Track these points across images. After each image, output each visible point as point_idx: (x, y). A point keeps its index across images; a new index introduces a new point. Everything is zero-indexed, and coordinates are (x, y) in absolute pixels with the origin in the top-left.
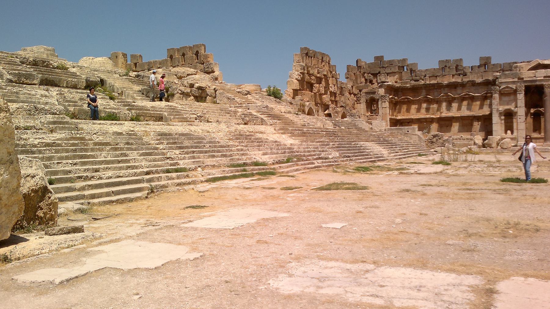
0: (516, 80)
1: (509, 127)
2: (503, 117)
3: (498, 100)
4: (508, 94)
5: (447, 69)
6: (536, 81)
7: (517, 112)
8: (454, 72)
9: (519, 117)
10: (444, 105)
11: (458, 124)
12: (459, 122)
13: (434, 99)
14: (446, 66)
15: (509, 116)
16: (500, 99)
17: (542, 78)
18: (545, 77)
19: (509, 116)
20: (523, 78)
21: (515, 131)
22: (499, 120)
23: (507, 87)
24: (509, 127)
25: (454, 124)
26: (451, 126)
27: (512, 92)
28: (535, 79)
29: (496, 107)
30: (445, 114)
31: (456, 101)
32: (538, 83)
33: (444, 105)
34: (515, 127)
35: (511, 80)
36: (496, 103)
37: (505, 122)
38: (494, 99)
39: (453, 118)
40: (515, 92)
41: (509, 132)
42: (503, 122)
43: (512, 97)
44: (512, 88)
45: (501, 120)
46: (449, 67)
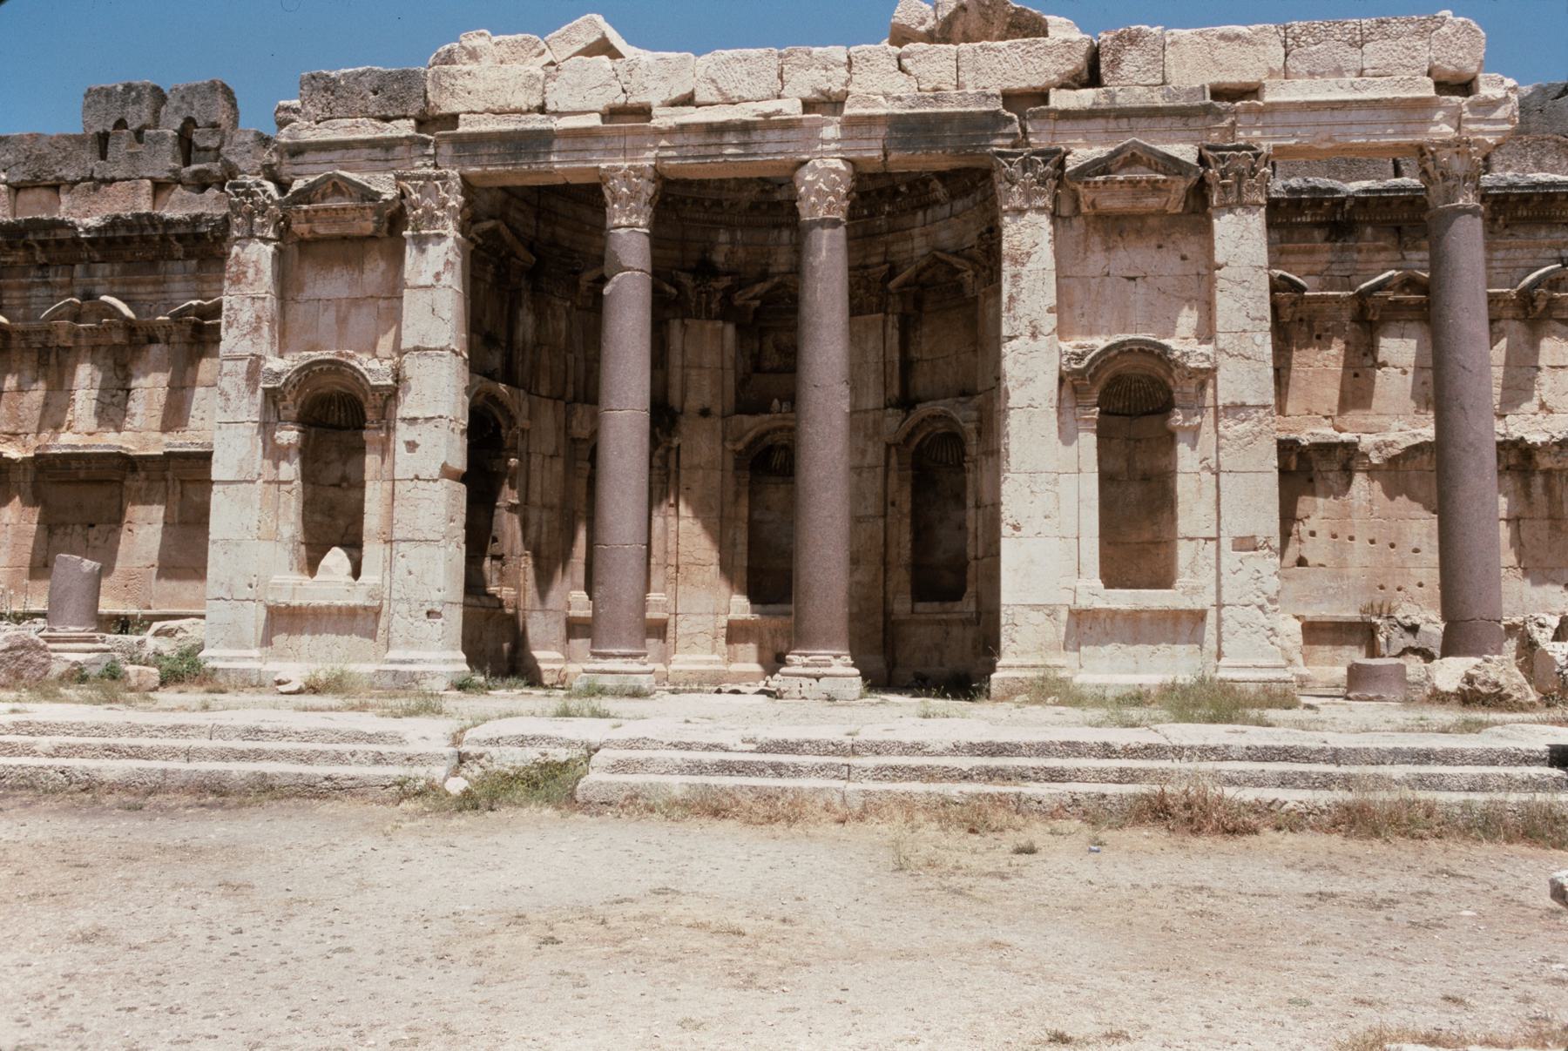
0: (405, 128)
1: (332, 523)
2: (289, 435)
3: (264, 283)
4: (346, 249)
5: (121, 147)
6: (541, 141)
7: (391, 395)
8: (165, 162)
9: (403, 433)
10: (86, 379)
11: (158, 512)
12: (165, 500)
13: (25, 335)
14: (121, 124)
15: (333, 424)
16: (286, 284)
17: (594, 121)
18: (612, 114)
19: (333, 424)
20: (453, 119)
21: (372, 551)
22: (260, 464)
23: (337, 186)
24: (332, 523)
25: (136, 512)
26: (117, 520)
27: (368, 227)
28: (536, 122)
29: (245, 347)
30: (81, 431)
31: (155, 351)
32: (560, 165)
33: (86, 379)
34: (372, 520)
35: (368, 130)
36: (246, 315)
37: (308, 477)
38: (237, 281)
39: (126, 464)
40: (393, 227)
41: (336, 559)
42: (290, 470)
43: (374, 272)
44: (368, 195)
45: (275, 453)
46: (139, 134)
